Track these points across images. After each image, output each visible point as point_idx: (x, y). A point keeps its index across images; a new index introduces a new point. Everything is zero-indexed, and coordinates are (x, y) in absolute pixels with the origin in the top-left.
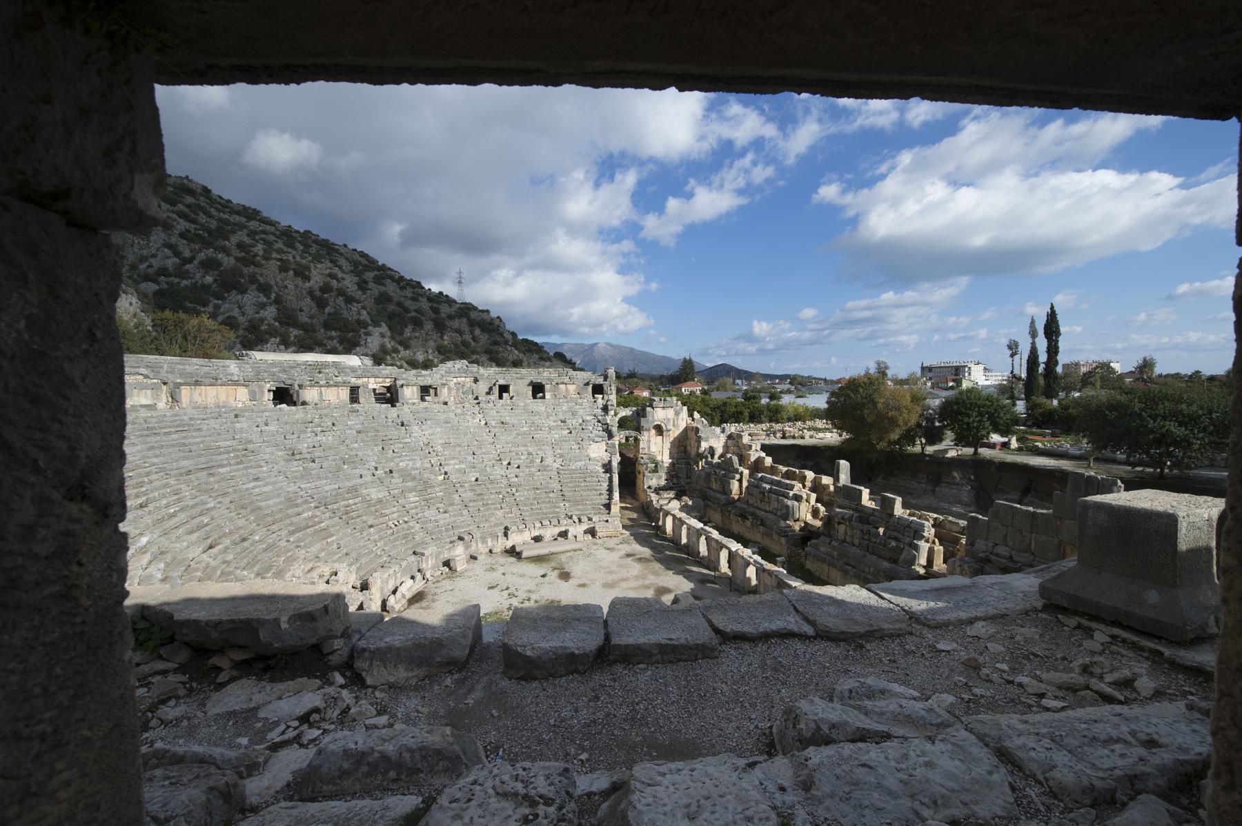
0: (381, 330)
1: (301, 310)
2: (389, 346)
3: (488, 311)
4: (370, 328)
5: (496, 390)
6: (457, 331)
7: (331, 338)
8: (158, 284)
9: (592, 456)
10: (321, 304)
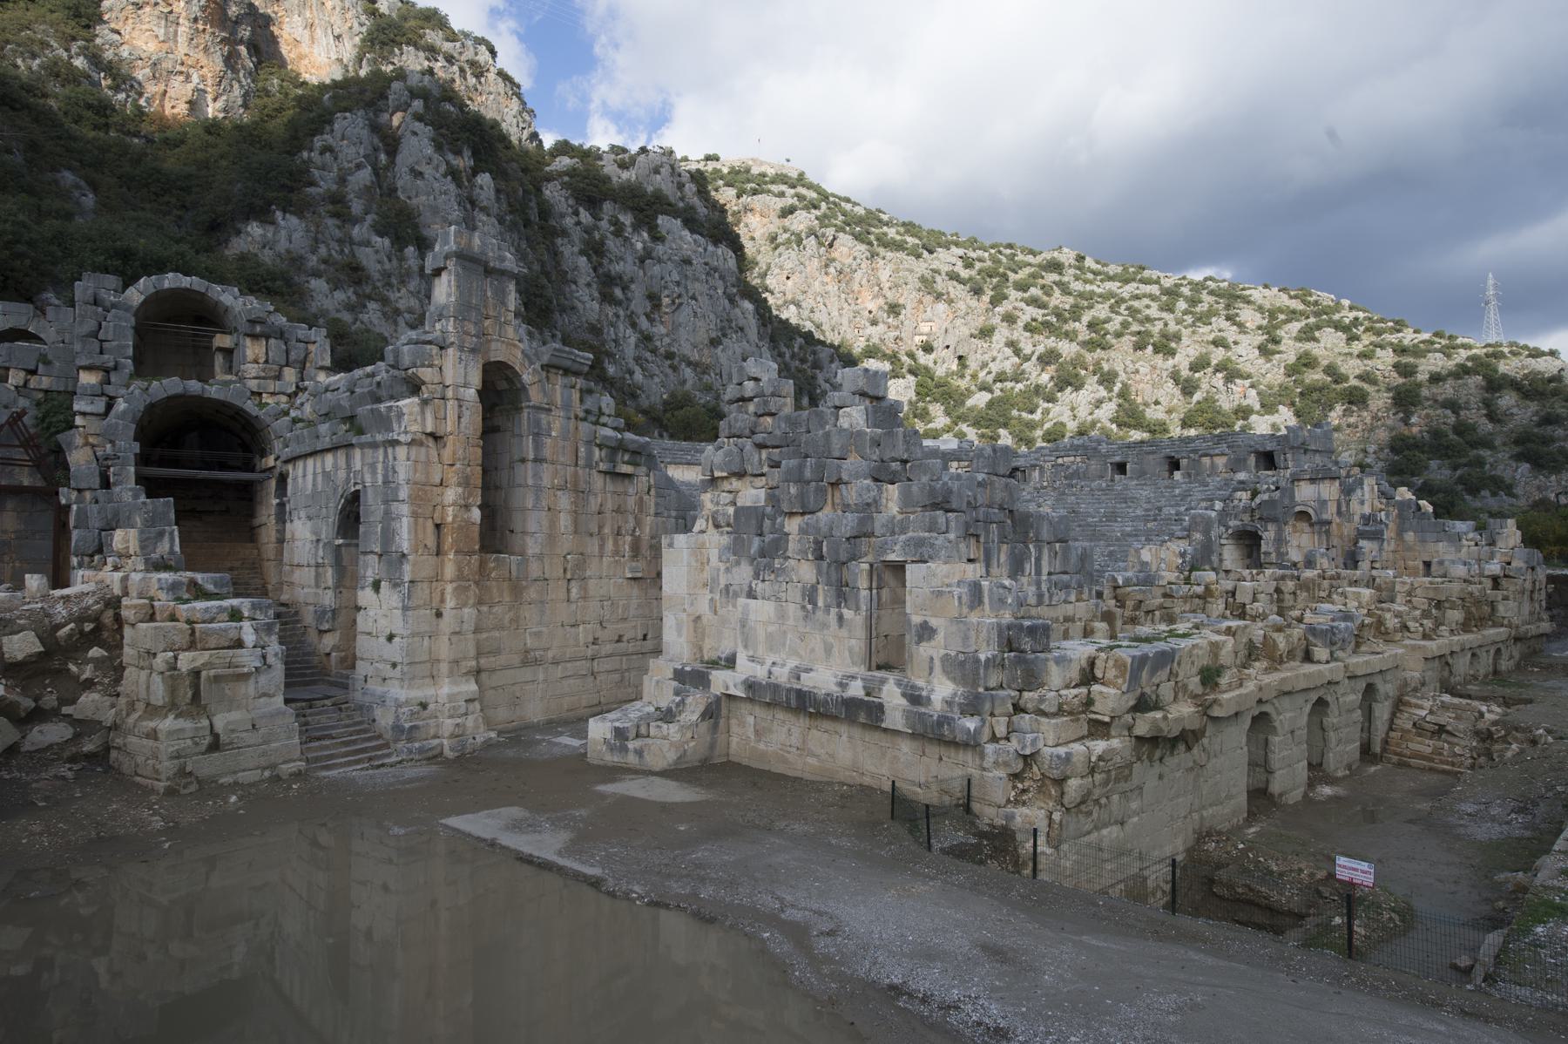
4: (1254, 418)
8: (991, 391)
10: (1188, 388)
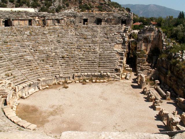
5: (83, 21)
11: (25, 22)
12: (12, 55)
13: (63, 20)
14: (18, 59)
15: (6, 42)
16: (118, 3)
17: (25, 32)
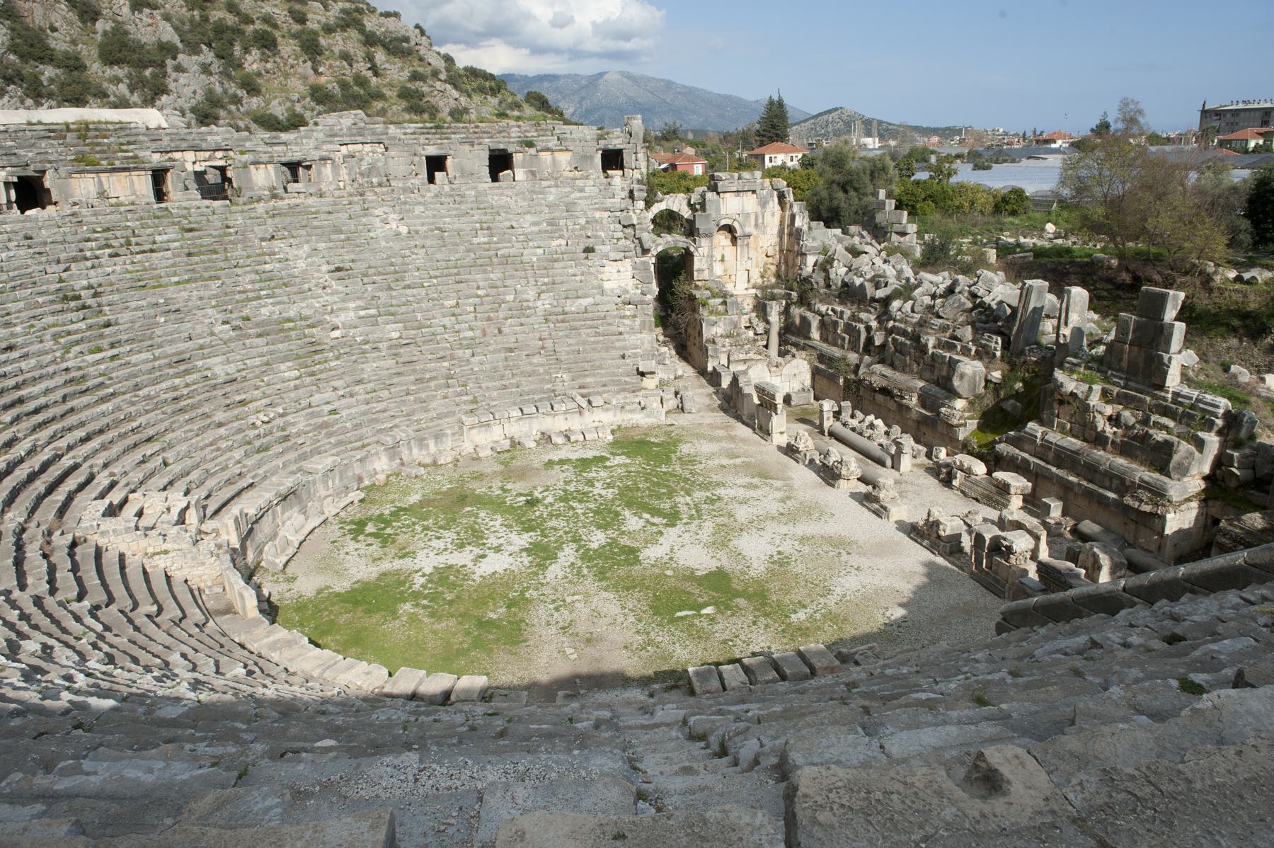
0: (201, 58)
1: (54, 29)
2: (218, 89)
3: (396, 15)
6: (346, 57)
7: (117, 80)
9: (607, 285)
11: (132, 182)
12: (134, 359)
13: (329, 166)
14: (168, 377)
15: (70, 294)
16: (489, 71)
17: (158, 238)
